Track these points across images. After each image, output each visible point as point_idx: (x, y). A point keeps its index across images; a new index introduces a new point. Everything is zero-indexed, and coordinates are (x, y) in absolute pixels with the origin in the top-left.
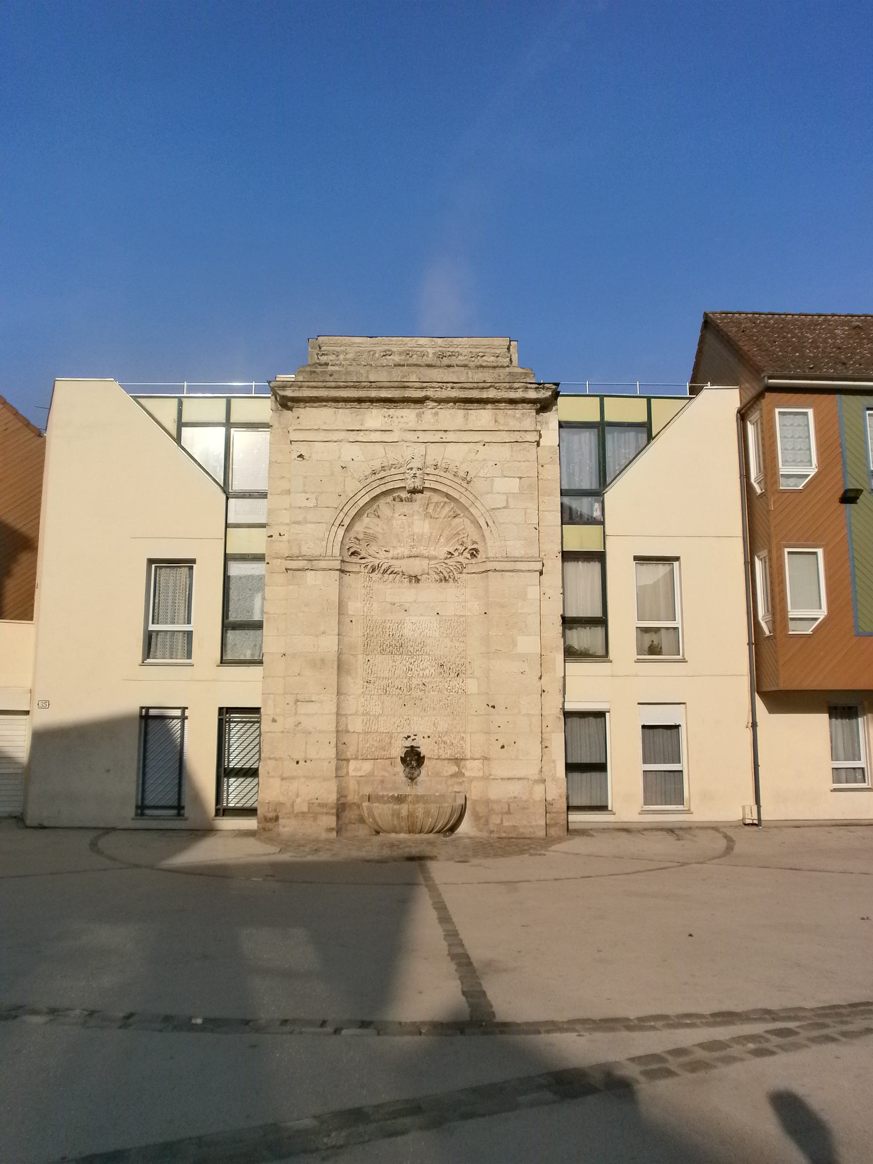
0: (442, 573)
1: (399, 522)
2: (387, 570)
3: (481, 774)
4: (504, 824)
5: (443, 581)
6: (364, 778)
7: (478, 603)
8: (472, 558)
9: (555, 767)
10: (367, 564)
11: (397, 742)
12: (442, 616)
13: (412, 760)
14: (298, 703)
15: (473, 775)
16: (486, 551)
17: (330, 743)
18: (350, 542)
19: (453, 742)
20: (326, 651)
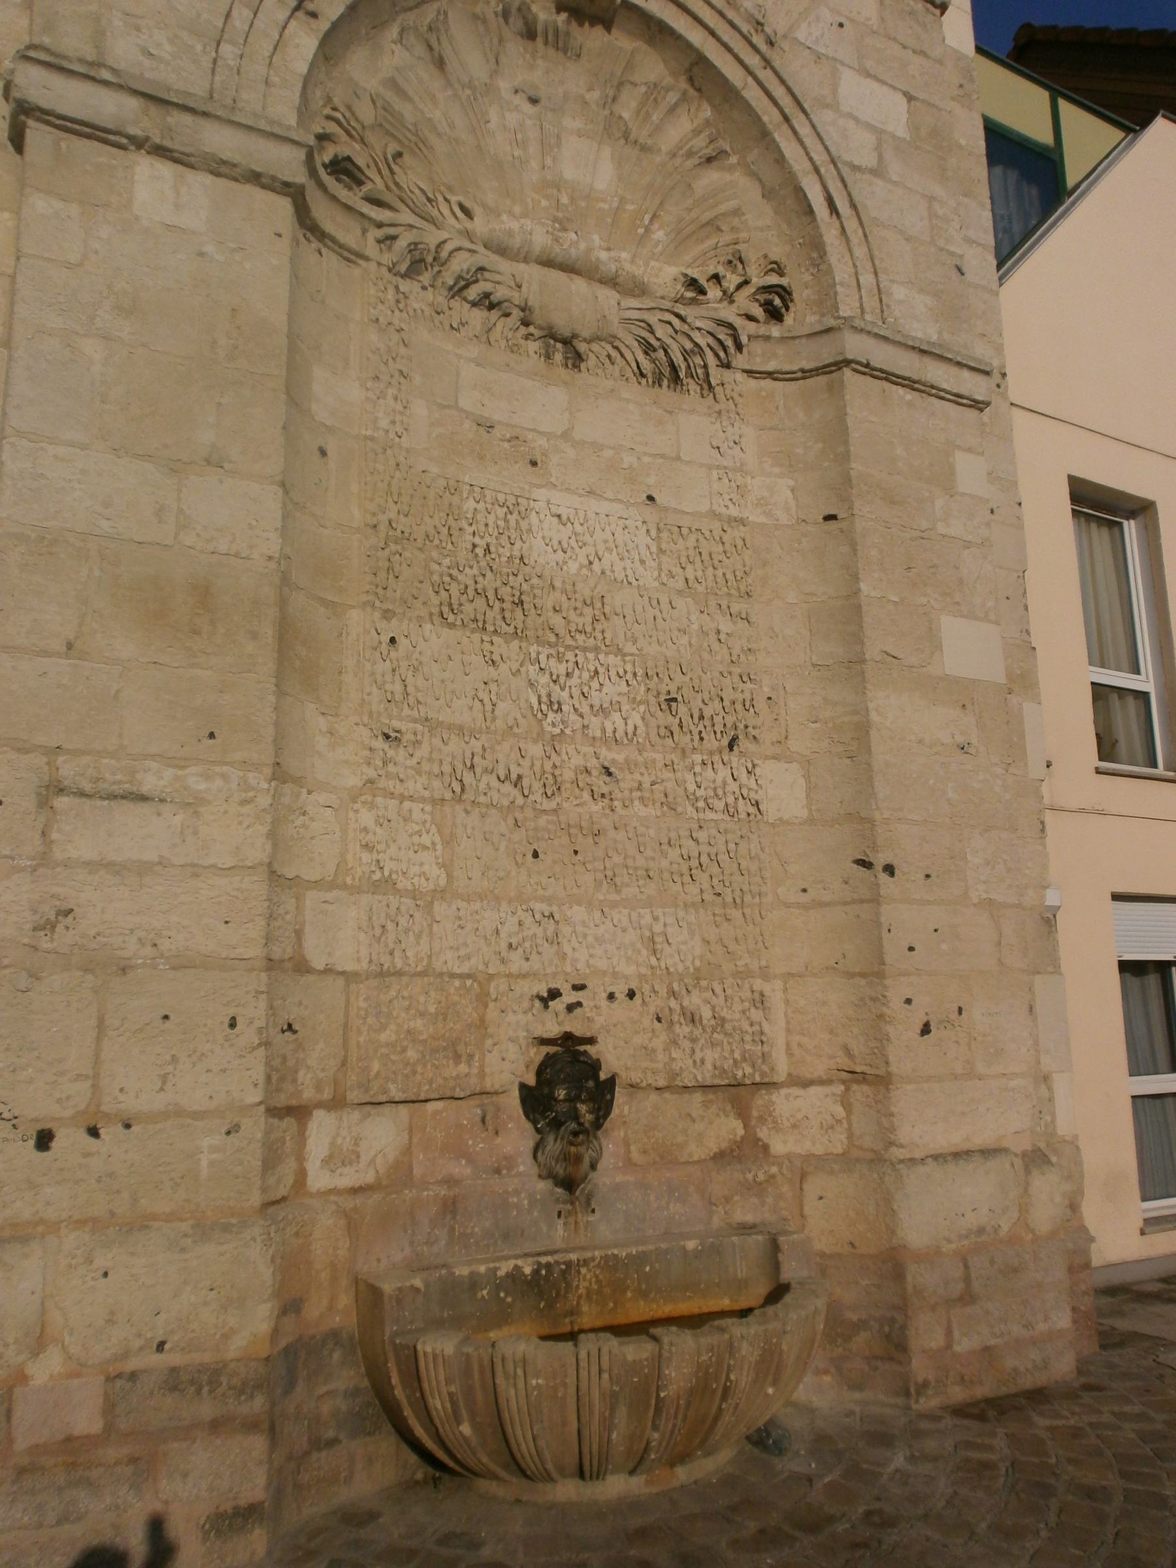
0: (666, 351)
1: (512, 119)
2: (466, 286)
3: (838, 1142)
4: (957, 1348)
5: (665, 383)
6: (377, 1196)
7: (792, 483)
8: (766, 322)
9: (1051, 1100)
10: (392, 231)
11: (511, 1018)
12: (666, 509)
13: (577, 1098)
14: (62, 802)
15: (798, 1150)
16: (827, 297)
17: (233, 1024)
18: (327, 111)
19: (725, 1013)
20: (223, 547)
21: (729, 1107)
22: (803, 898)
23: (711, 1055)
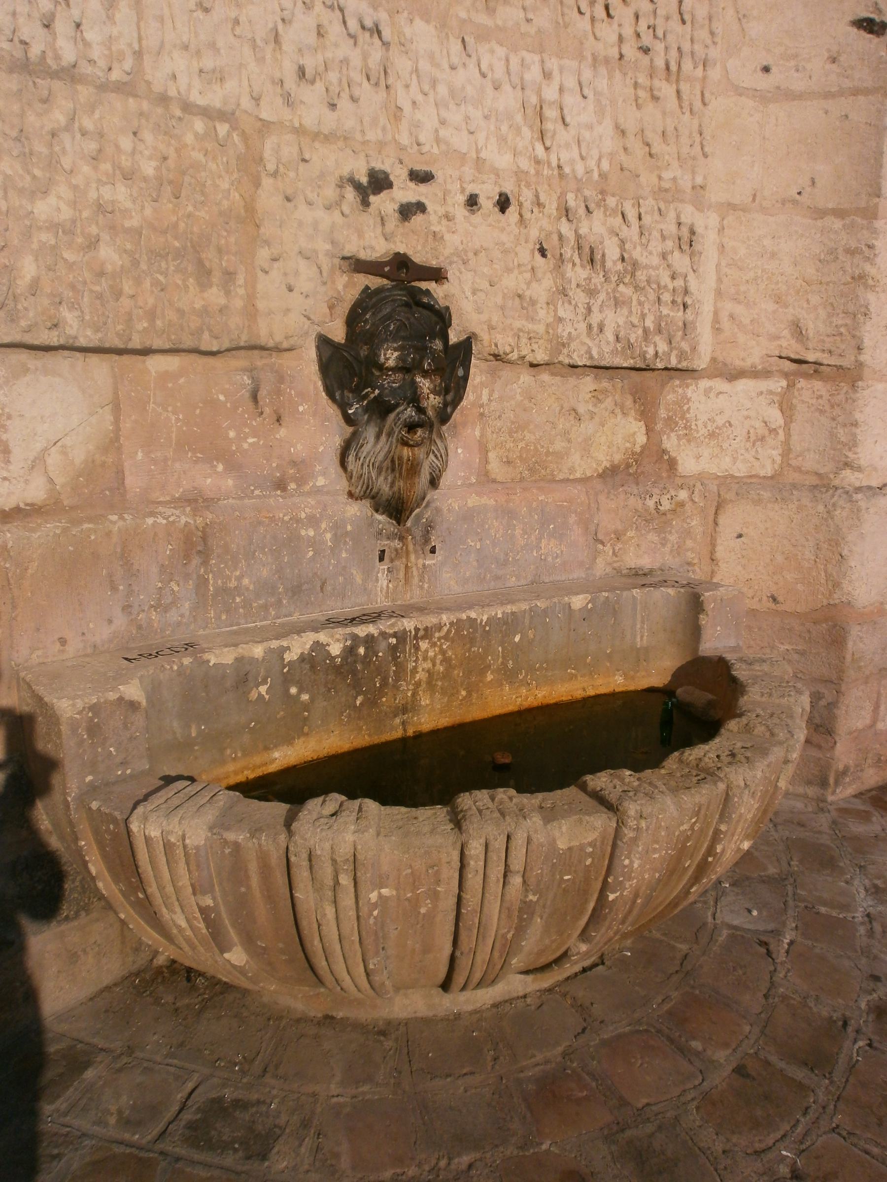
6: (51, 527)
11: (303, 212)
19: (637, 254)
21: (629, 402)
22: (764, 82)
23: (613, 319)
